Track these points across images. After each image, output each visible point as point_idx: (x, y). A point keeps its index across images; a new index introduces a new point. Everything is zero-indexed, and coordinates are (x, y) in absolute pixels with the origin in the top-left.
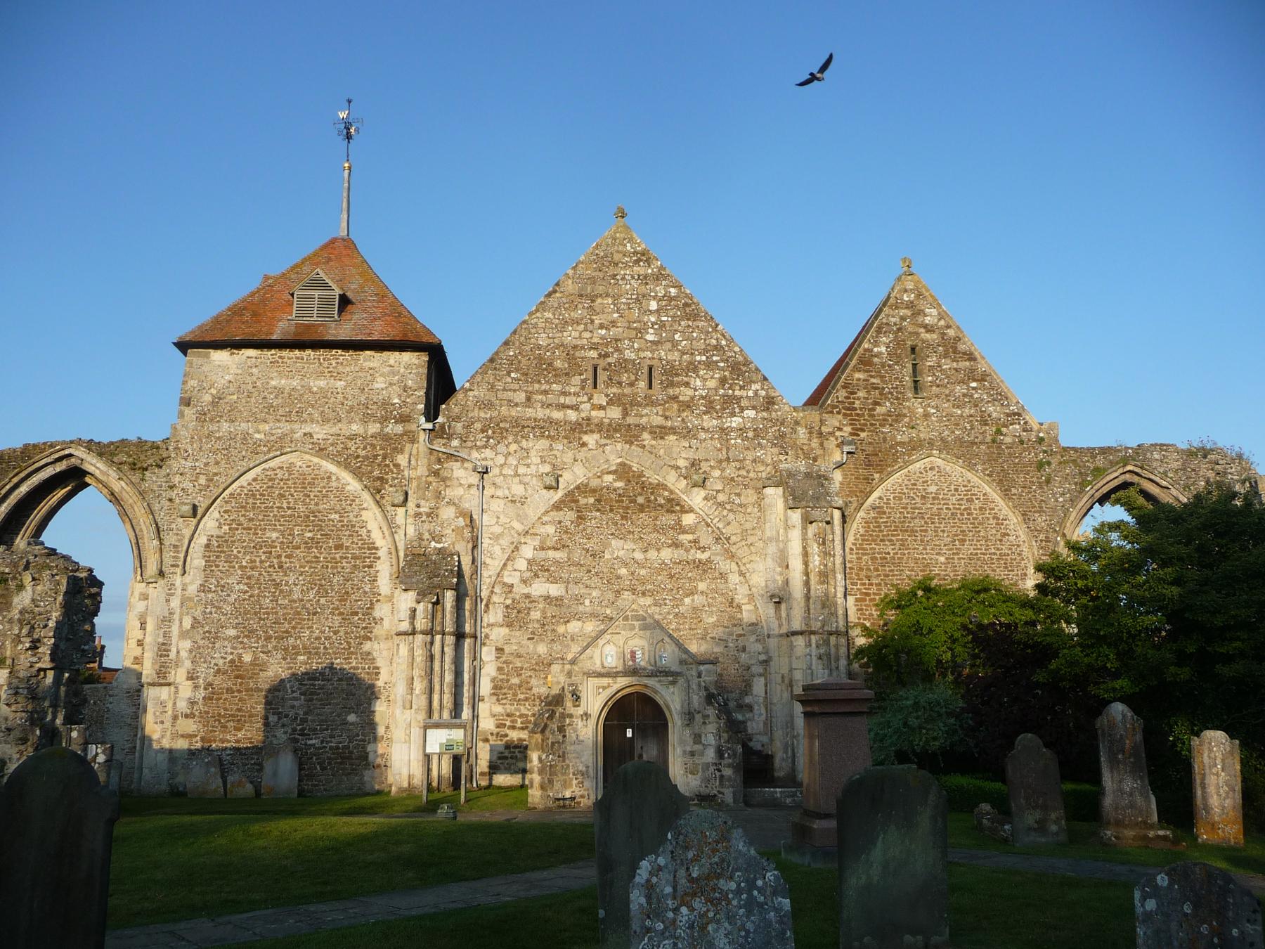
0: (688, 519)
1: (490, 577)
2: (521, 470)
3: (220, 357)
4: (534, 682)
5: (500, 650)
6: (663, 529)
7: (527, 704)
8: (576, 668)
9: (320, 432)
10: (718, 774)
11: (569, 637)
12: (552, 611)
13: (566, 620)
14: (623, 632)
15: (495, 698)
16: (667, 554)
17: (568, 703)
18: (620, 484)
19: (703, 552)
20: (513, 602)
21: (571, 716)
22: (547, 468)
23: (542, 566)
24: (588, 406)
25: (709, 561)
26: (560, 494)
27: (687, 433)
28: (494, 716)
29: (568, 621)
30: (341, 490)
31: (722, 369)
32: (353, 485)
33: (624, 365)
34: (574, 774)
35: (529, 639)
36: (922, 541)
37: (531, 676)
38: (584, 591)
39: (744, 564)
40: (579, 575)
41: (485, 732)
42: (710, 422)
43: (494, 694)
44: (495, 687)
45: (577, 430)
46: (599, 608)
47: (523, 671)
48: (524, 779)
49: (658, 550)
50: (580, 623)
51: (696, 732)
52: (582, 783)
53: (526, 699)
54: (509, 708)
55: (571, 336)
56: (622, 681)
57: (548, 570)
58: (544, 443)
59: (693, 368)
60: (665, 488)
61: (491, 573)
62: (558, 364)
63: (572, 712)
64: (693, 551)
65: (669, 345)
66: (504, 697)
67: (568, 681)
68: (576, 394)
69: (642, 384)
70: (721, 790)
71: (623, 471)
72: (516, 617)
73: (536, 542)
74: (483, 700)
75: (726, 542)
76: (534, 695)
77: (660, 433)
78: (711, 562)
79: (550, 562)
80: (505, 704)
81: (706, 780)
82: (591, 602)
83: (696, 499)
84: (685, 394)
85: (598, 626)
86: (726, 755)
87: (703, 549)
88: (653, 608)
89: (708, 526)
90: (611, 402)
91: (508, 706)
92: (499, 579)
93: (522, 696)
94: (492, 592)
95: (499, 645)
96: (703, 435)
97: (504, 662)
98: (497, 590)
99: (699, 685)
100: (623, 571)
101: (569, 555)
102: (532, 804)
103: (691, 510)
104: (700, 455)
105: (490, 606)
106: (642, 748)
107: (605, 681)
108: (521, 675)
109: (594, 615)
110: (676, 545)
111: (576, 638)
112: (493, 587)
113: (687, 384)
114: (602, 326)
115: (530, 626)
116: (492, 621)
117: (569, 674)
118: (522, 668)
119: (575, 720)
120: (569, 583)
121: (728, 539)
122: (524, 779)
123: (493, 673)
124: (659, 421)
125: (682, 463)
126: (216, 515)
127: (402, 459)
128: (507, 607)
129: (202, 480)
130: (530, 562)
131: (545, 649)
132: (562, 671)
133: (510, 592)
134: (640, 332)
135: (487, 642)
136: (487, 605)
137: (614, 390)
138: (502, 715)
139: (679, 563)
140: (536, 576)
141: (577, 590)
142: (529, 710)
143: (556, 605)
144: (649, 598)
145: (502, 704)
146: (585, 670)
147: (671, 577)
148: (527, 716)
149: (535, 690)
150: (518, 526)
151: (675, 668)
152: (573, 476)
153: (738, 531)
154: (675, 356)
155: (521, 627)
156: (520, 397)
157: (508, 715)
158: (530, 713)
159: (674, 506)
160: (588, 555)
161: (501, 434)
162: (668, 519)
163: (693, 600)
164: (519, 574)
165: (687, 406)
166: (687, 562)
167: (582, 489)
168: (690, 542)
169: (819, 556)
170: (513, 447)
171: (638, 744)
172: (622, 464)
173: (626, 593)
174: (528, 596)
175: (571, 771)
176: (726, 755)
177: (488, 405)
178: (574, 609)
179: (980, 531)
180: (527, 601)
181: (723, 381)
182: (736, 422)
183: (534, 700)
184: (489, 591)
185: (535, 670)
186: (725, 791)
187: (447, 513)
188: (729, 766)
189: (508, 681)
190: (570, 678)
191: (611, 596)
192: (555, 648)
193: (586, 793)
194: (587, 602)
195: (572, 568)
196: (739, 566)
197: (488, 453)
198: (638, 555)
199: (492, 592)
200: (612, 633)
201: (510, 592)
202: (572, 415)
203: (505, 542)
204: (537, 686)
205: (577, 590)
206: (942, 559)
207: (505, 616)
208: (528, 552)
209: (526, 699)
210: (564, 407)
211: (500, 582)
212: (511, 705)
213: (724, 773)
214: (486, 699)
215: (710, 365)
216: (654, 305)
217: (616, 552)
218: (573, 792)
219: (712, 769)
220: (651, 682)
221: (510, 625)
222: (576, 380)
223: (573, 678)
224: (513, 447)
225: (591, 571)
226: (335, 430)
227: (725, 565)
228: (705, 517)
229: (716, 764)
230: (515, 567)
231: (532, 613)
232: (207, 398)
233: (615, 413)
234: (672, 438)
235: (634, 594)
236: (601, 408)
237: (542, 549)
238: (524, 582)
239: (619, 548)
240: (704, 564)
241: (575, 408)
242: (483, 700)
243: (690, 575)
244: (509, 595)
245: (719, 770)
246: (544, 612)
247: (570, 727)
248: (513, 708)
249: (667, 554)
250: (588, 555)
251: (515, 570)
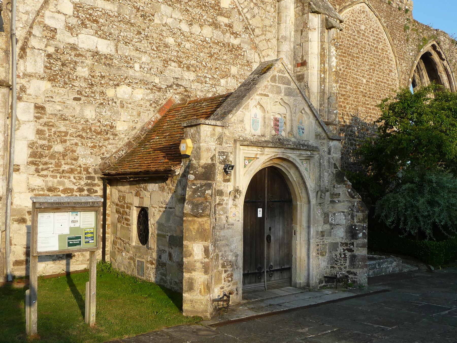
1: (27, 13)
4: (80, 150)
5: (40, 109)
6: (205, 6)
7: (72, 176)
8: (227, 132)
10: (348, 254)
11: (118, 102)
12: (100, 70)
13: (115, 83)
14: (270, 95)
15: (33, 168)
17: (219, 177)
19: (236, 37)
20: (57, 51)
21: (220, 193)
23: (90, 15)
25: (239, 47)
28: (33, 190)
29: (118, 85)
34: (223, 266)
35: (75, 99)
36: (357, 65)
37: (76, 144)
38: (134, 53)
39: (264, 57)
40: (130, 35)
41: (20, 211)
43: (32, 163)
44: (33, 155)
46: (148, 75)
47: (68, 137)
48: (68, 264)
49: (201, 26)
50: (129, 89)
51: (326, 210)
52: (232, 275)
53: (72, 171)
54: (52, 182)
57: (97, 22)
61: (28, 8)
63: (221, 188)
64: (228, 35)
66: (44, 167)
67: (219, 148)
70: (353, 270)
72: (61, 70)
74: (18, 170)
75: (252, 33)
76: (80, 166)
78: (241, 49)
79: (99, 13)
80: (46, 176)
81: (333, 262)
82: (141, 67)
85: (147, 95)
86: (361, 235)
87: (236, 35)
88: (196, 84)
89: (240, 14)
91: (49, 179)
92: (39, 19)
93: (66, 167)
94: (30, 33)
95: (40, 102)
97: (46, 124)
98: (36, 31)
99: (329, 162)
100: (170, 41)
101: (119, 9)
102: (191, 312)
105: (28, 51)
106: (270, 229)
107: (253, 151)
108: (65, 141)
109: (144, 82)
110: (215, 25)
111: (126, 105)
112: (31, 27)
115: (76, 83)
116: (30, 70)
117: (220, 140)
118: (66, 134)
119: (225, 198)
120: (119, 41)
121: (253, 30)
122: (68, 264)
123: (32, 137)
128: (49, 56)
131: (94, 113)
132: (213, 135)
133: (53, 38)
135: (25, 97)
136: (23, 49)
138: (43, 189)
139: (217, 44)
140: (84, 25)
141: (128, 51)
142: (74, 184)
143: (105, 64)
144: (192, 73)
145: (42, 176)
146: (236, 136)
147: (211, 56)
148: (72, 190)
149: (81, 161)
151: (312, 142)
153: (260, 26)
155: (66, 84)
157: (50, 190)
158: (75, 188)
160: (139, 14)
163: (227, 82)
164: (63, 18)
166: (224, 44)
168: (226, 25)
169: (336, 58)
171: (267, 225)
173: (173, 64)
174: (74, 48)
175: (221, 262)
176: (361, 235)
178: (125, 72)
179: (381, 65)
180: (73, 53)
183: (80, 173)
184: (25, 31)
185: (82, 137)
186: (358, 271)
188: (363, 246)
189: (50, 147)
190: (221, 144)
191: (159, 64)
192: (104, 114)
193: (234, 287)
194: (137, 66)
195: (122, 26)
196: (260, 58)
198: (184, 27)
199: (30, 33)
200: (261, 94)
201: (53, 38)
204: (84, 156)
205: (128, 51)
206: (365, 81)
207: (46, 67)
209: (72, 171)
211: (40, 23)
212: (53, 177)
213: (356, 253)
214: (22, 168)
217: (165, 18)
218: (222, 288)
219: (340, 249)
220: (292, 156)
221: (52, 79)
223: (224, 145)
225: (141, 33)
227: (251, 54)
228: (238, 5)
229: (346, 244)
230: (59, 8)
231: (79, 69)
235: (180, 66)
240: (236, 50)
242: (18, 170)
243: (225, 57)
244: (51, 42)
245: (351, 250)
246: (92, 70)
247: (220, 207)
248: (55, 180)
249: (208, 32)
250: (139, 14)
251: (59, 12)
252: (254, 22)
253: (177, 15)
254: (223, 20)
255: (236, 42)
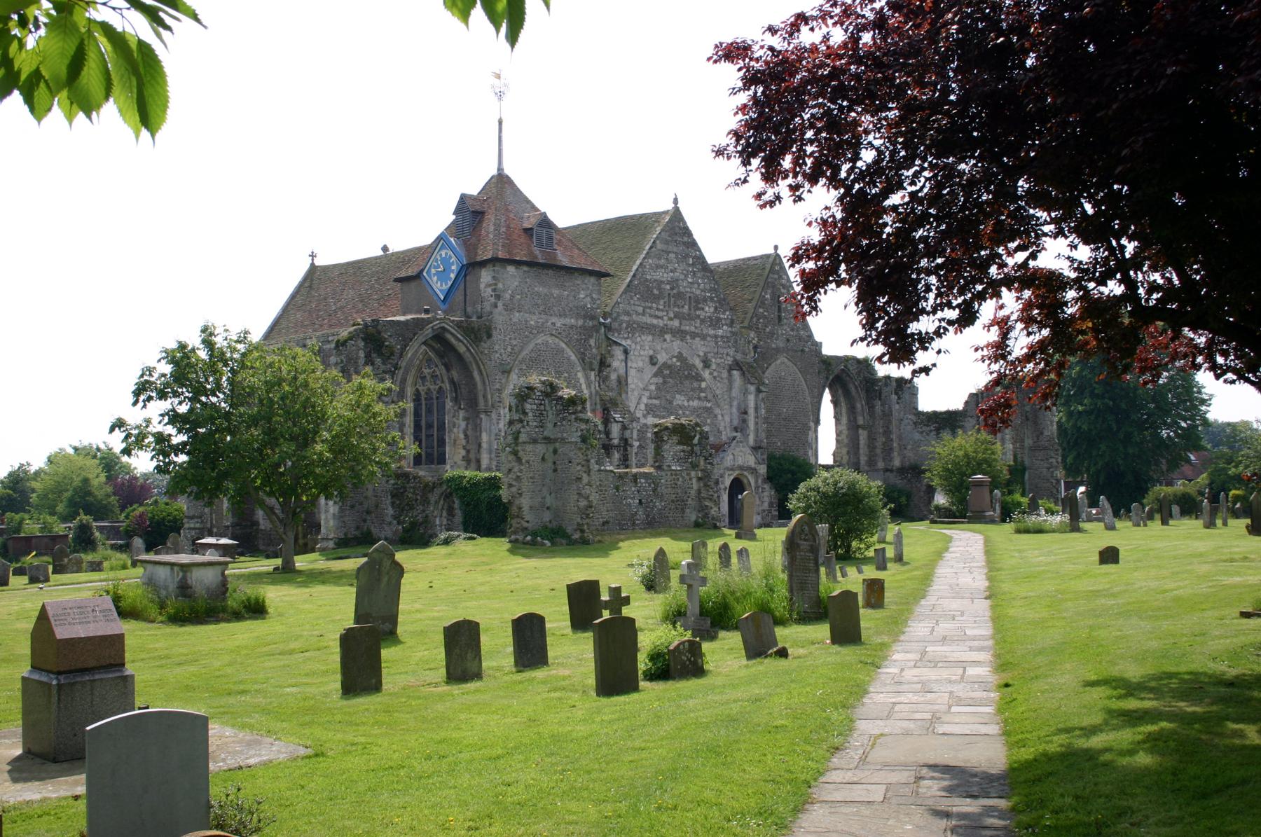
0: (703, 385)
2: (642, 353)
3: (511, 269)
9: (559, 322)
16: (695, 403)
18: (678, 364)
22: (651, 353)
24: (665, 318)
26: (655, 369)
27: (704, 337)
30: (569, 359)
31: (715, 302)
32: (573, 357)
33: (680, 295)
42: (712, 332)
45: (663, 331)
55: (660, 275)
56: (737, 472)
58: (650, 338)
59: (705, 300)
60: (694, 366)
62: (656, 292)
65: (696, 286)
68: (662, 310)
69: (687, 307)
71: (680, 357)
73: (647, 394)
77: (694, 335)
83: (706, 374)
84: (702, 314)
87: (709, 401)
90: (675, 317)
96: (709, 339)
103: (704, 380)
104: (708, 350)
110: (699, 398)
113: (703, 309)
114: (671, 271)
124: (693, 329)
125: (702, 354)
126: (516, 371)
127: (592, 342)
129: (509, 350)
130: (646, 405)
134: (686, 276)
137: (676, 309)
140: (649, 413)
150: (641, 386)
152: (662, 358)
154: (698, 292)
156: (640, 309)
159: (699, 378)
161: (633, 331)
162: (696, 385)
165: (703, 321)
167: (665, 365)
170: (639, 339)
172: (679, 353)
174: (645, 425)
177: (627, 313)
181: (716, 308)
182: (720, 332)
187: (613, 377)
197: (629, 342)
202: (661, 323)
203: (636, 393)
208: (645, 400)
210: (657, 317)
215: (711, 298)
216: (691, 262)
222: (662, 302)
224: (639, 339)
226: (564, 322)
232: (507, 296)
233: (676, 323)
234: (698, 339)
236: (671, 319)
237: (650, 398)
238: (645, 416)
239: (680, 400)
241: (661, 318)
249: (695, 403)
252: (717, 392)
253: (683, 398)
254: (703, 395)
255: (709, 405)
